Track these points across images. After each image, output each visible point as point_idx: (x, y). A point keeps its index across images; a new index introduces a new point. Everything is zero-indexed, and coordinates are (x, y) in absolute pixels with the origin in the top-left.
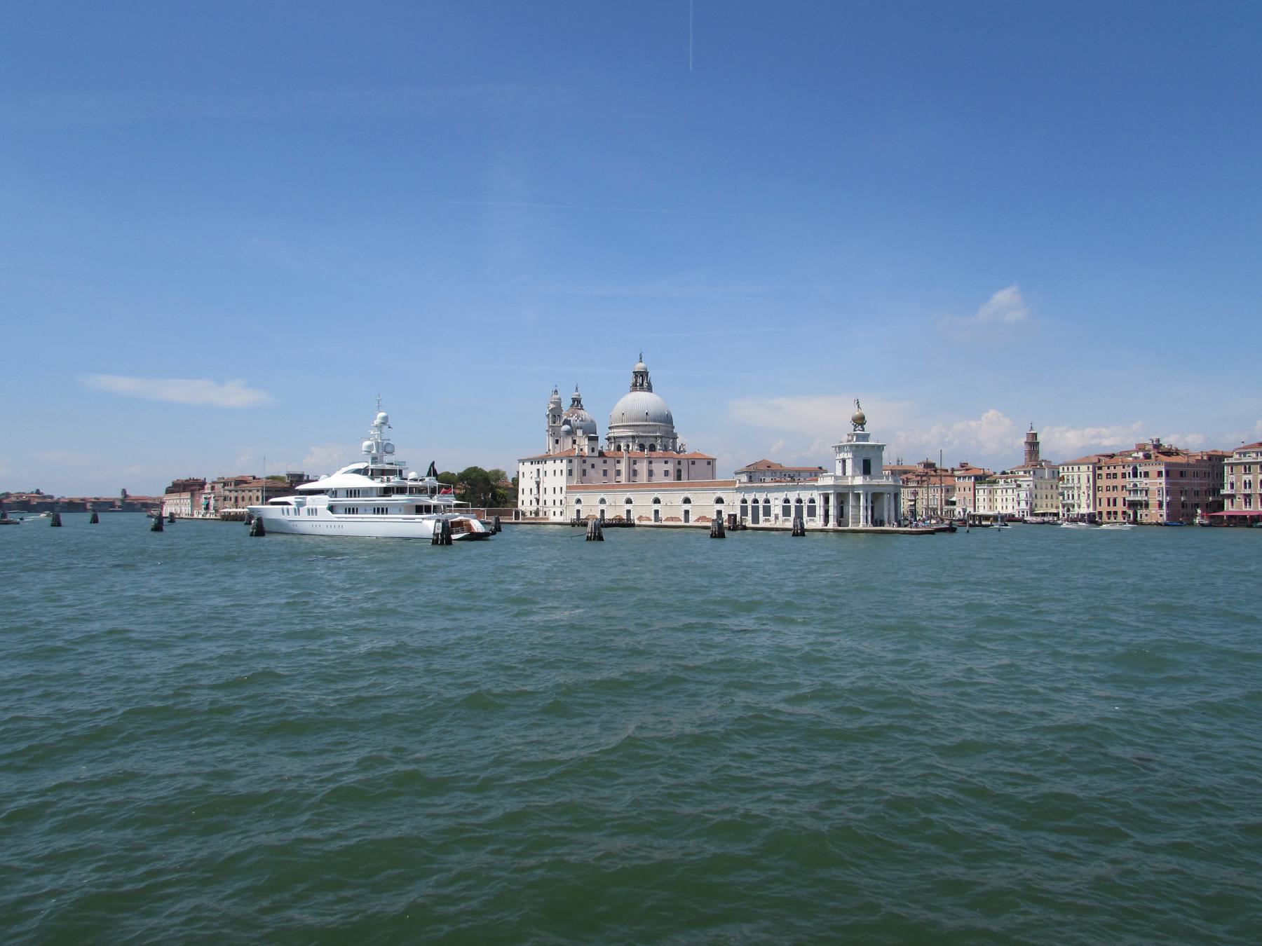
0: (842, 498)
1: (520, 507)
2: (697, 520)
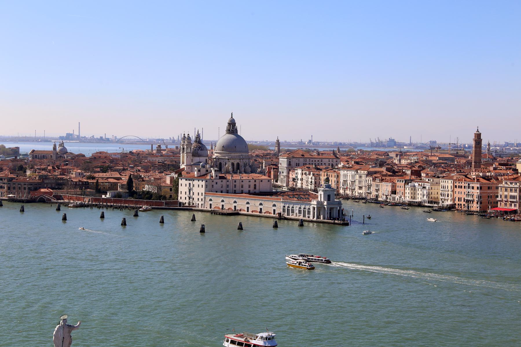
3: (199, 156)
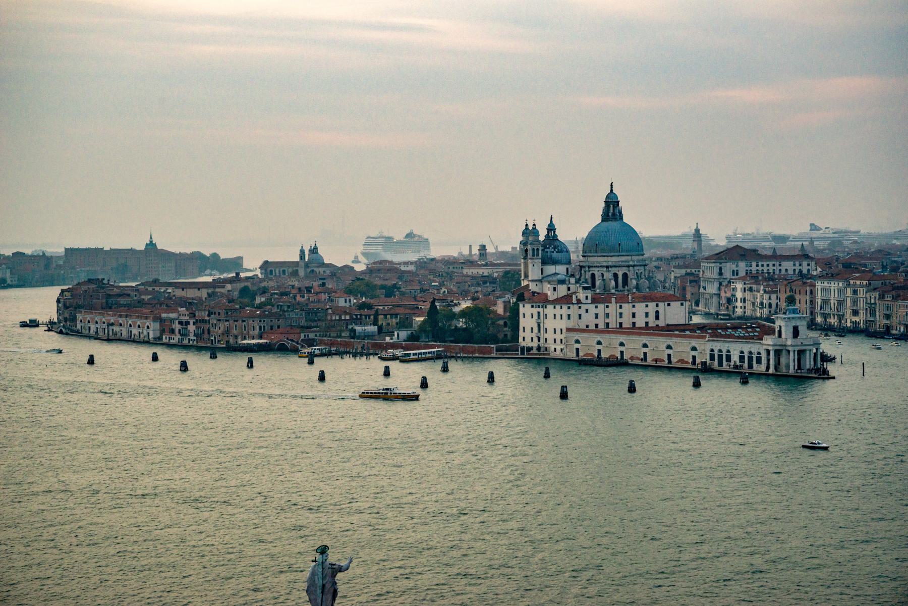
0: (778, 353)
1: (522, 343)
2: (678, 362)
3: (555, 262)
